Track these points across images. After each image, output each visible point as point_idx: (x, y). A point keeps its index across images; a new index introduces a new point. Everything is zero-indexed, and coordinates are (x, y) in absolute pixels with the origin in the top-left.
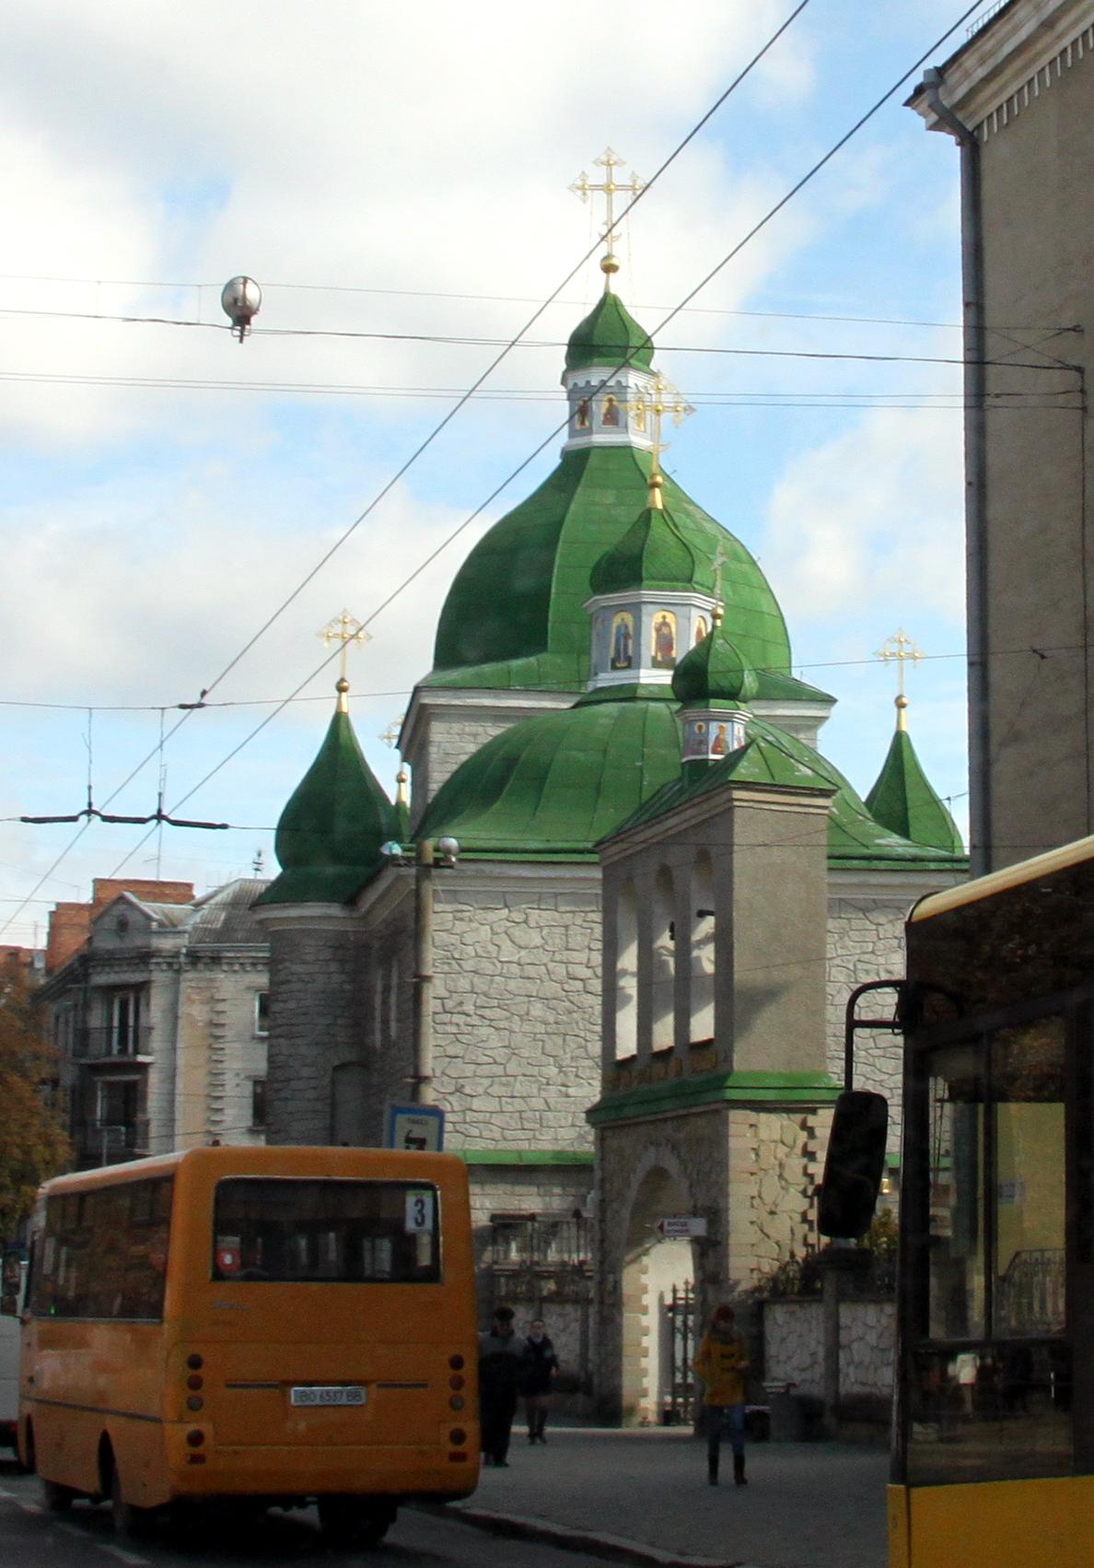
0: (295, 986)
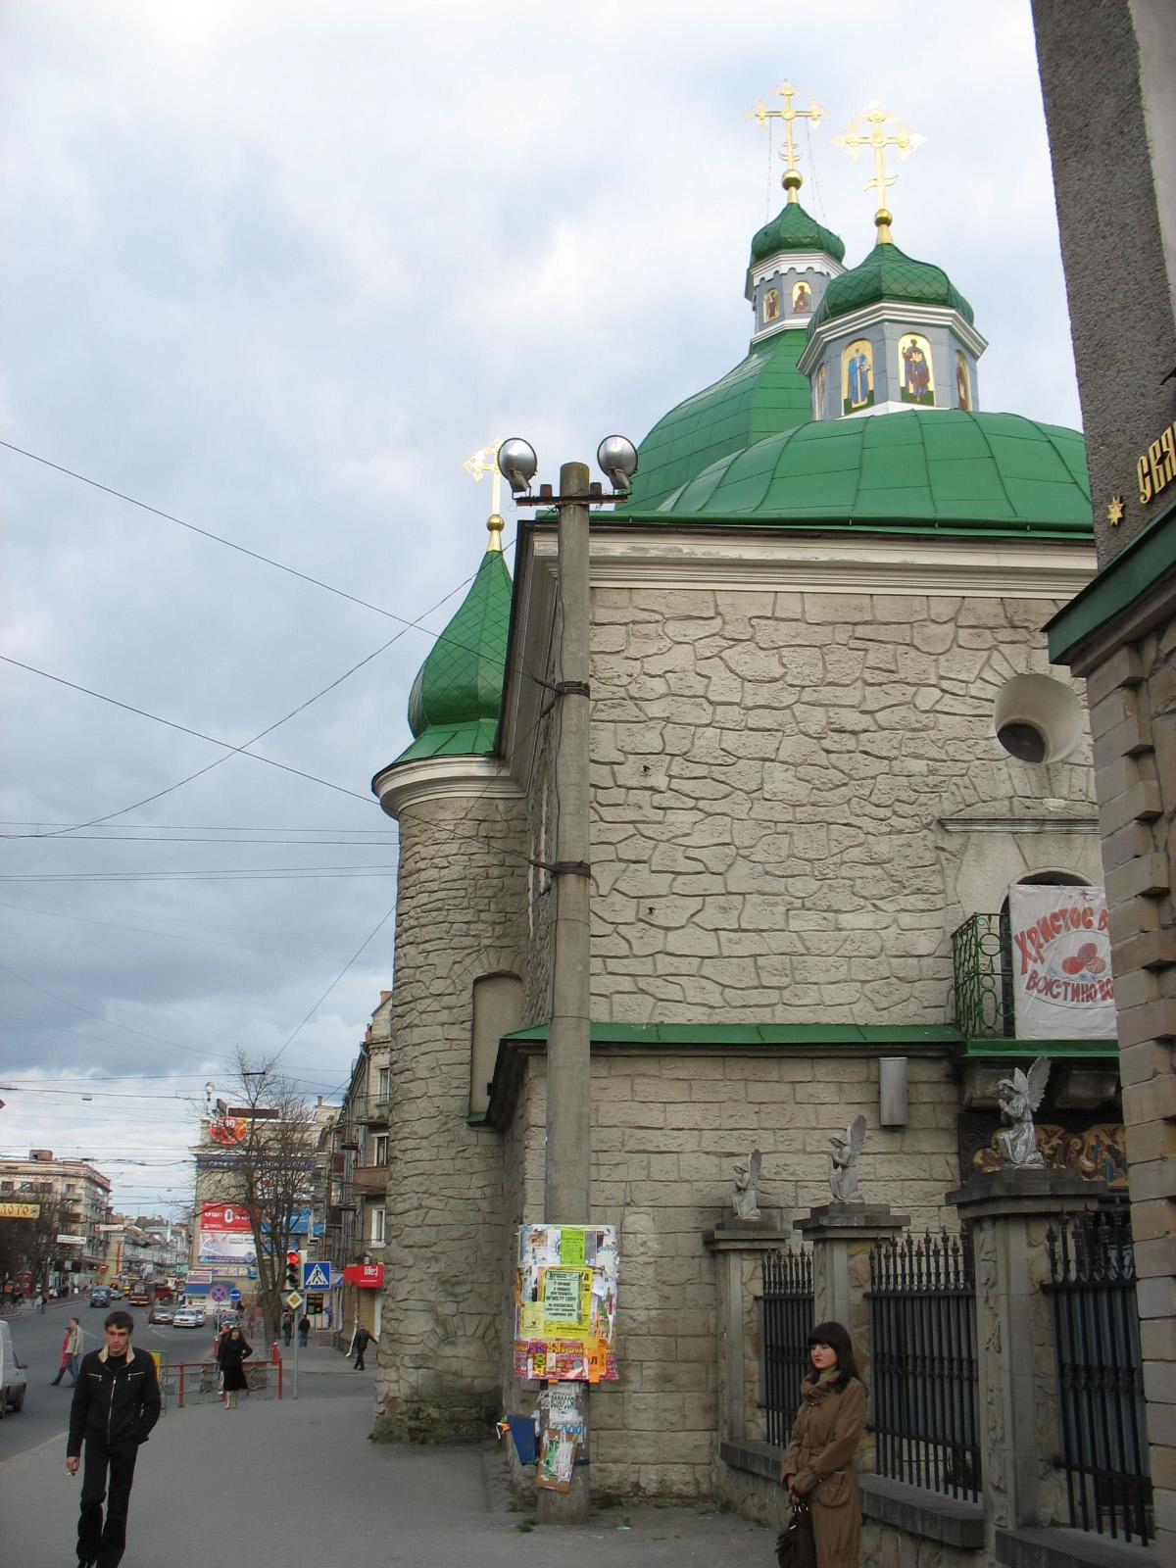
0: (424, 876)
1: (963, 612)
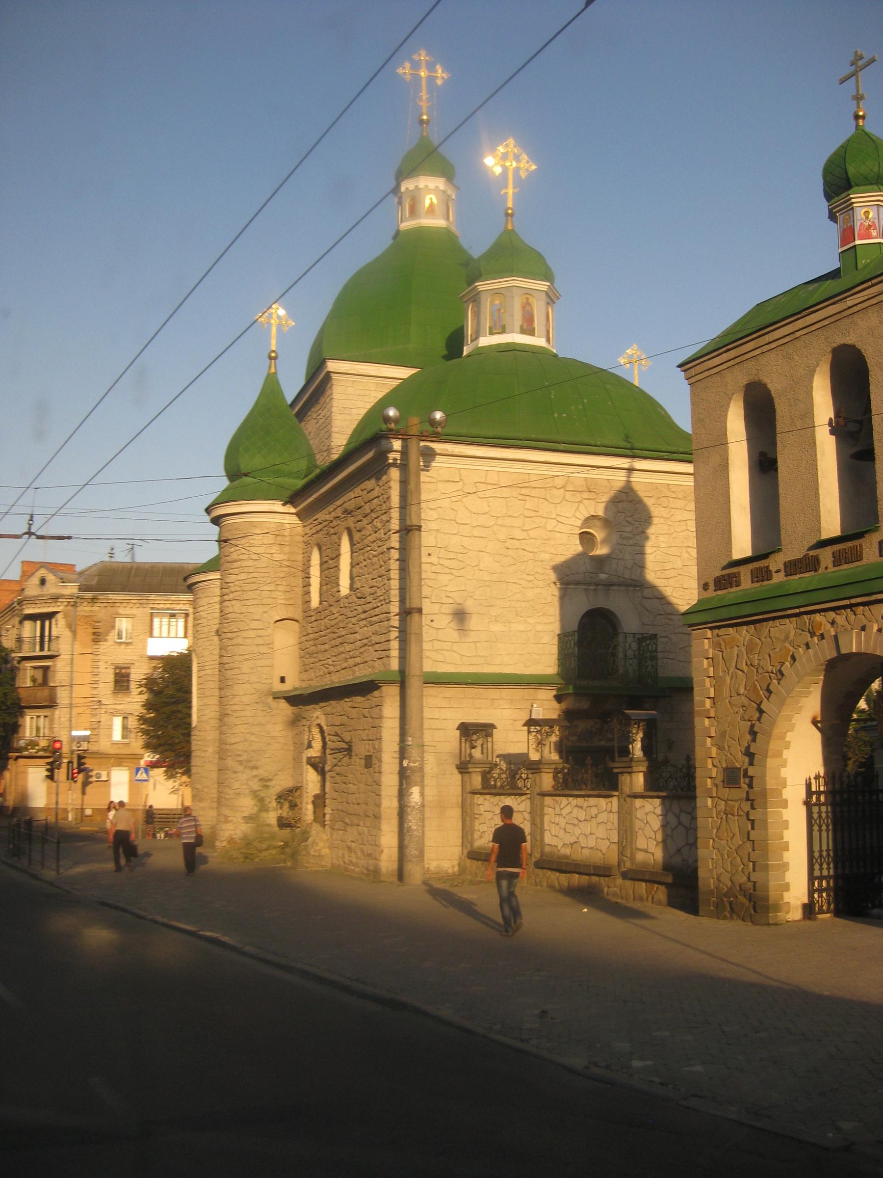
0: (244, 564)
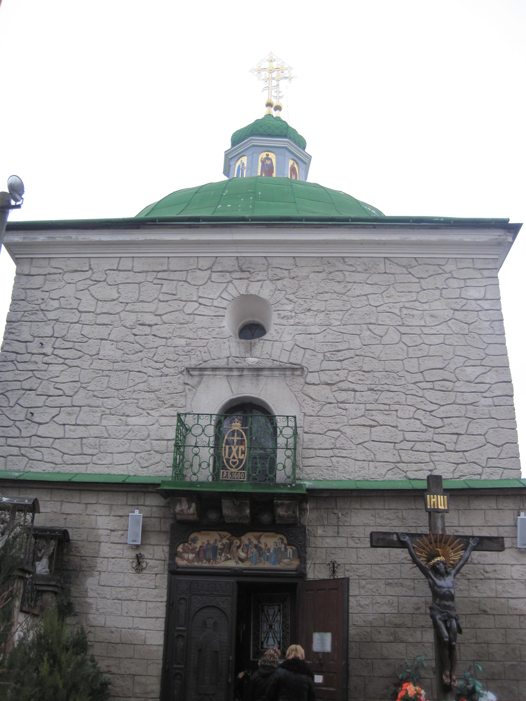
1: (216, 264)
